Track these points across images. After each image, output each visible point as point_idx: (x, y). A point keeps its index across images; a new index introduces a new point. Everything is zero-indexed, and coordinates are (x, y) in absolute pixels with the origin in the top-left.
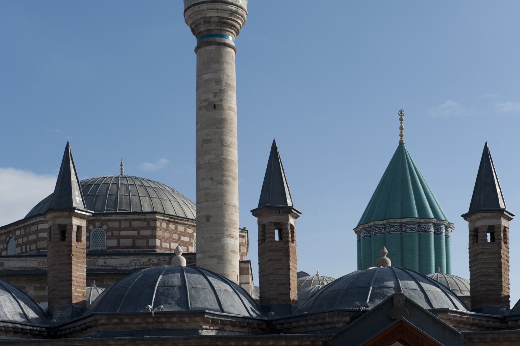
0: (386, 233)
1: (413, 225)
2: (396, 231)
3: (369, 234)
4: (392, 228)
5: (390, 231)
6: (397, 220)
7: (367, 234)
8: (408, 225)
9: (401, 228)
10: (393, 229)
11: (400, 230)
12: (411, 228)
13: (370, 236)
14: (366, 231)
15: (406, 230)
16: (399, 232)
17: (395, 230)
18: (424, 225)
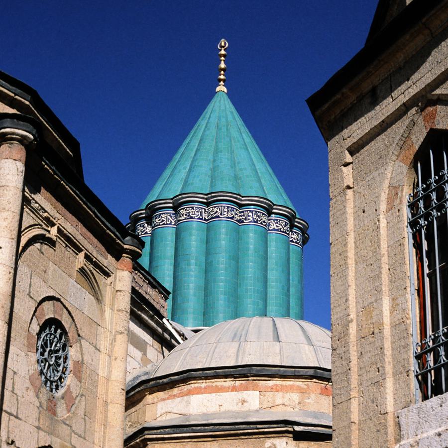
1: (191, 207)
2: (164, 224)
10: (160, 220)
11: (171, 222)
15: (180, 218)
16: (170, 224)
17: (163, 221)
18: (214, 207)
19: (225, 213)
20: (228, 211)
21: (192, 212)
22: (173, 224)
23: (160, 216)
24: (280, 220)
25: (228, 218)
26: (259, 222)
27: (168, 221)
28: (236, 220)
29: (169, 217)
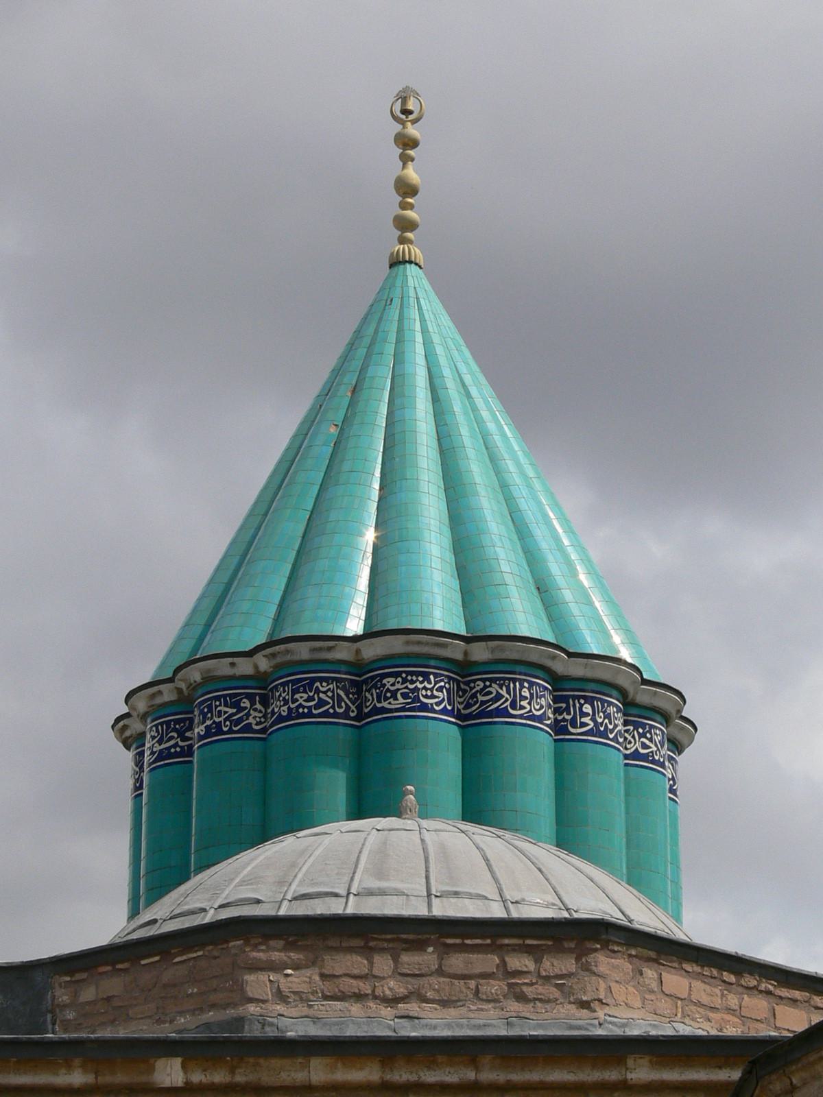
0: (271, 726)
3: (185, 739)
4: (301, 697)
5: (289, 708)
6: (330, 649)
7: (172, 743)
8: (397, 675)
9: (359, 692)
10: (310, 699)
14: (168, 723)
15: (385, 704)
16: (345, 715)
17: (322, 703)
18: (492, 680)
19: (524, 703)
20: (531, 695)
21: (425, 688)
22: (352, 715)
24: (652, 727)
25: (532, 718)
26: (611, 736)
27: (340, 707)
28: (547, 725)
29: (342, 693)
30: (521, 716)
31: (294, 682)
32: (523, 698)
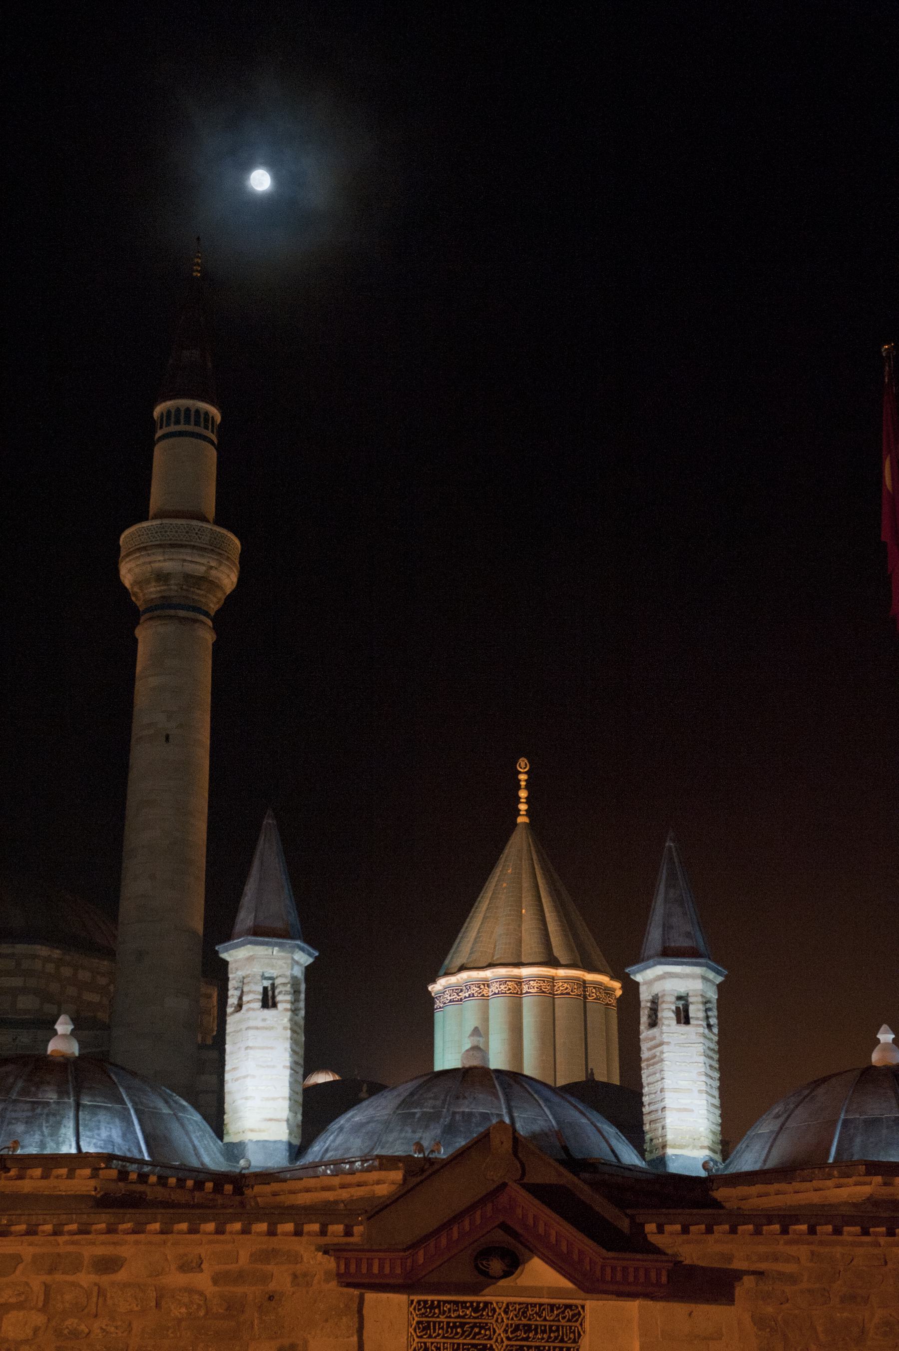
2: (510, 993)
4: (502, 987)
7: (454, 997)
9: (521, 985)
10: (506, 988)
11: (518, 991)
12: (540, 988)
13: (461, 1000)
14: (453, 990)
16: (517, 994)
19: (575, 990)
22: (519, 993)
23: (506, 983)
29: (516, 986)
30: (574, 995)
31: (500, 981)
32: (575, 989)
